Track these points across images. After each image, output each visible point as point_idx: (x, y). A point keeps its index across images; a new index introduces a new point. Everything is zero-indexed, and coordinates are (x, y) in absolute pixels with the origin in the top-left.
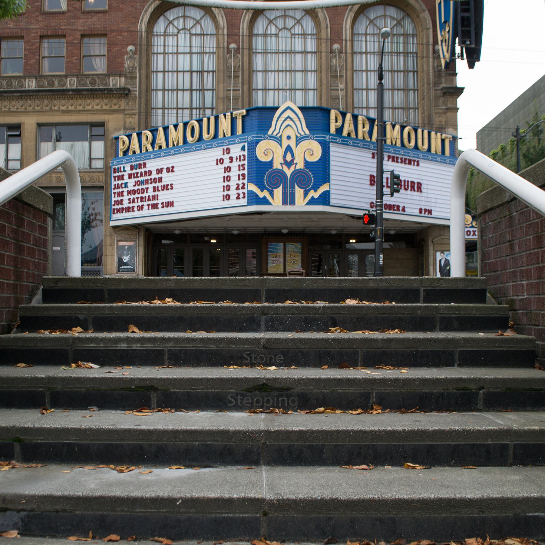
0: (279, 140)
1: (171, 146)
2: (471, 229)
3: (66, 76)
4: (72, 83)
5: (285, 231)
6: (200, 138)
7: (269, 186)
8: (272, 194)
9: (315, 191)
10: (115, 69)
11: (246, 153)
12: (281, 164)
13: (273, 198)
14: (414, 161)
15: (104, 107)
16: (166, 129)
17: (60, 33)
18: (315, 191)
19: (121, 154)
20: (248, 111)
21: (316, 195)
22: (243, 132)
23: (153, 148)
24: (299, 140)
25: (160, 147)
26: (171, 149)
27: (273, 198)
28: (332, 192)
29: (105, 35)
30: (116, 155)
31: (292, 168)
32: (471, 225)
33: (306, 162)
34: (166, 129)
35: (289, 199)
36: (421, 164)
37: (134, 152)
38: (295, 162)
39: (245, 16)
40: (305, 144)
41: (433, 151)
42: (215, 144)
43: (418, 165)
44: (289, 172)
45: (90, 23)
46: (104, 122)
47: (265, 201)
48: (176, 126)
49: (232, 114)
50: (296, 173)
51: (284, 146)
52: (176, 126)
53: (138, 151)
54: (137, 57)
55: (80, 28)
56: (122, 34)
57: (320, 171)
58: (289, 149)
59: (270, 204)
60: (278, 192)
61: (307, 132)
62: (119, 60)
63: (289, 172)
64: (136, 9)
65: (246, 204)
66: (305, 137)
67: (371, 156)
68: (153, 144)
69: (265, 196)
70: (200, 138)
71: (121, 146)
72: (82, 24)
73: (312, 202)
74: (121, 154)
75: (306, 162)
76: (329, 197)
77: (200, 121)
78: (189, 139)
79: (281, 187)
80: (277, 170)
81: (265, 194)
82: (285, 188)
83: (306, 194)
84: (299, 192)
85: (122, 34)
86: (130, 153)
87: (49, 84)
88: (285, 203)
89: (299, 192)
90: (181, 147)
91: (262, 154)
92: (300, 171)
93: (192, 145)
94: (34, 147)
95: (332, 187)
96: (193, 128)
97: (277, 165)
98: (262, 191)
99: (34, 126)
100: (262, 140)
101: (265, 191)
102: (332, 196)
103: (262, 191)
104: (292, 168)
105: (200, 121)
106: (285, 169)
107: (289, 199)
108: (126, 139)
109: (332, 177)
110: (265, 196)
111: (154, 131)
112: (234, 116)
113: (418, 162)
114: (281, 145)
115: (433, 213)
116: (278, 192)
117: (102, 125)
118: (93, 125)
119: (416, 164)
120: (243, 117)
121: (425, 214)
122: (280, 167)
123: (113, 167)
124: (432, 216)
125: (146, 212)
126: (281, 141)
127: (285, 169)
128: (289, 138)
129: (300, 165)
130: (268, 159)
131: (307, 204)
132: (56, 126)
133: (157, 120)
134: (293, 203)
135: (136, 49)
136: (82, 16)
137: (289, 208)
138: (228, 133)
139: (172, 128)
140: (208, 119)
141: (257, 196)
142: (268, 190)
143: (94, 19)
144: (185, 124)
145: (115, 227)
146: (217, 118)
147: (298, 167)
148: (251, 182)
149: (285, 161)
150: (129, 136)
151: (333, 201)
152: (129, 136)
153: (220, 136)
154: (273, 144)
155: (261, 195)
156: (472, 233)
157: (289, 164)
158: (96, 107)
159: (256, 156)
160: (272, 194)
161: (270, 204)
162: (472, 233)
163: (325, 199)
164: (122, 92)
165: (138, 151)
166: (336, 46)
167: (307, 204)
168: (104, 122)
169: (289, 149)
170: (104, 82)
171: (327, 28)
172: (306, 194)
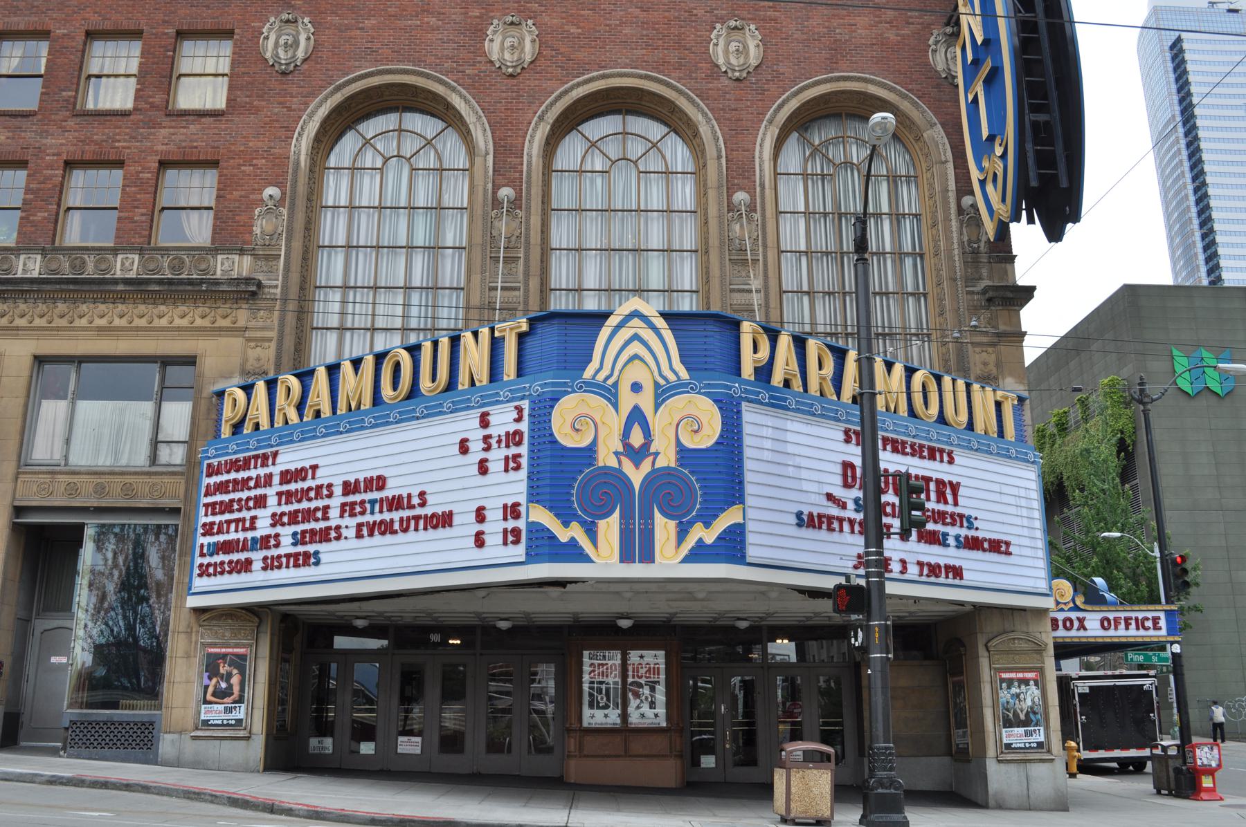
0: (610, 393)
1: (342, 409)
2: (1073, 615)
3: (115, 251)
4: (127, 266)
5: (625, 624)
6: (414, 392)
7: (585, 511)
8: (591, 532)
9: (707, 525)
10: (231, 234)
11: (524, 426)
12: (616, 453)
13: (594, 542)
14: (941, 451)
15: (199, 322)
16: (333, 370)
17: (112, 157)
18: (707, 525)
19: (226, 431)
20: (532, 322)
21: (710, 537)
22: (520, 373)
23: (301, 416)
24: (663, 394)
25: (318, 414)
26: (343, 417)
27: (594, 542)
28: (750, 526)
29: (213, 164)
30: (217, 434)
31: (646, 466)
32: (1071, 605)
33: (682, 451)
34: (333, 370)
35: (637, 546)
36: (957, 459)
37: (257, 426)
38: (652, 450)
39: (535, 130)
40: (678, 404)
41: (979, 427)
42: (447, 404)
44: (636, 476)
45: (183, 137)
46: (195, 357)
47: (573, 552)
48: (357, 363)
49: (492, 330)
50: (656, 478)
51: (626, 406)
52: (357, 363)
53: (265, 424)
54: (285, 211)
55: (160, 148)
56: (255, 162)
57: (717, 475)
58: (637, 416)
59: (586, 559)
60: (610, 527)
61: (684, 374)
62: (243, 218)
63: (636, 476)
64: (289, 109)
65: (523, 559)
66: (678, 388)
67: (842, 436)
68: (300, 408)
69: (573, 539)
70: (414, 392)
71: (227, 412)
72: (165, 139)
73: (700, 553)
74: (226, 431)
75: (682, 451)
76: (743, 542)
77: (414, 350)
78: (387, 391)
79: (616, 514)
80: (607, 471)
81: (576, 532)
82: (626, 518)
83: (682, 534)
84: (664, 528)
85: (255, 162)
86: (248, 429)
87: (73, 267)
88: (626, 556)
89: (664, 528)
90: (366, 412)
91: (569, 430)
92: (667, 471)
93: (392, 407)
94: (20, 410)
95: (751, 514)
96: (397, 366)
97: (606, 457)
98: (566, 524)
99: (27, 362)
100: (567, 393)
101: (574, 524)
102: (750, 538)
103: (566, 524)
104: (646, 466)
105: (414, 350)
106: (628, 468)
107: (637, 546)
108: (240, 395)
109: (749, 489)
110: (573, 539)
111: (305, 376)
112: (497, 334)
113: (950, 454)
114: (616, 406)
115: (965, 574)
116: (610, 527)
117: (190, 361)
118: (166, 361)
119: (946, 458)
120: (521, 337)
121: (947, 577)
122: (612, 462)
123: (207, 462)
124: (963, 583)
125: (257, 576)
126: (616, 395)
127: (628, 468)
128: (636, 387)
129: (667, 459)
130: (584, 442)
131: (686, 560)
132: (80, 362)
133: (324, 349)
134: (648, 556)
135: (284, 194)
136: (166, 122)
137: (637, 570)
138: (483, 377)
139: (347, 367)
140: (435, 344)
141: (553, 537)
142: (583, 523)
143: (193, 128)
144: (380, 358)
145: (199, 611)
146: (455, 341)
147: (660, 463)
148: (538, 502)
149: (627, 445)
150: (248, 389)
151: (752, 553)
152: (248, 389)
153: (463, 383)
154: (595, 404)
155: (563, 535)
156: (1076, 624)
157: (637, 455)
158: (178, 322)
159: (552, 435)
160: (591, 532)
161: (586, 559)
162: (1076, 624)
163: (732, 546)
164: (243, 287)
165: (265, 424)
166: (740, 196)
167: (686, 560)
168: (195, 357)
169: (637, 416)
170: (203, 267)
171: (719, 157)
172: (682, 534)
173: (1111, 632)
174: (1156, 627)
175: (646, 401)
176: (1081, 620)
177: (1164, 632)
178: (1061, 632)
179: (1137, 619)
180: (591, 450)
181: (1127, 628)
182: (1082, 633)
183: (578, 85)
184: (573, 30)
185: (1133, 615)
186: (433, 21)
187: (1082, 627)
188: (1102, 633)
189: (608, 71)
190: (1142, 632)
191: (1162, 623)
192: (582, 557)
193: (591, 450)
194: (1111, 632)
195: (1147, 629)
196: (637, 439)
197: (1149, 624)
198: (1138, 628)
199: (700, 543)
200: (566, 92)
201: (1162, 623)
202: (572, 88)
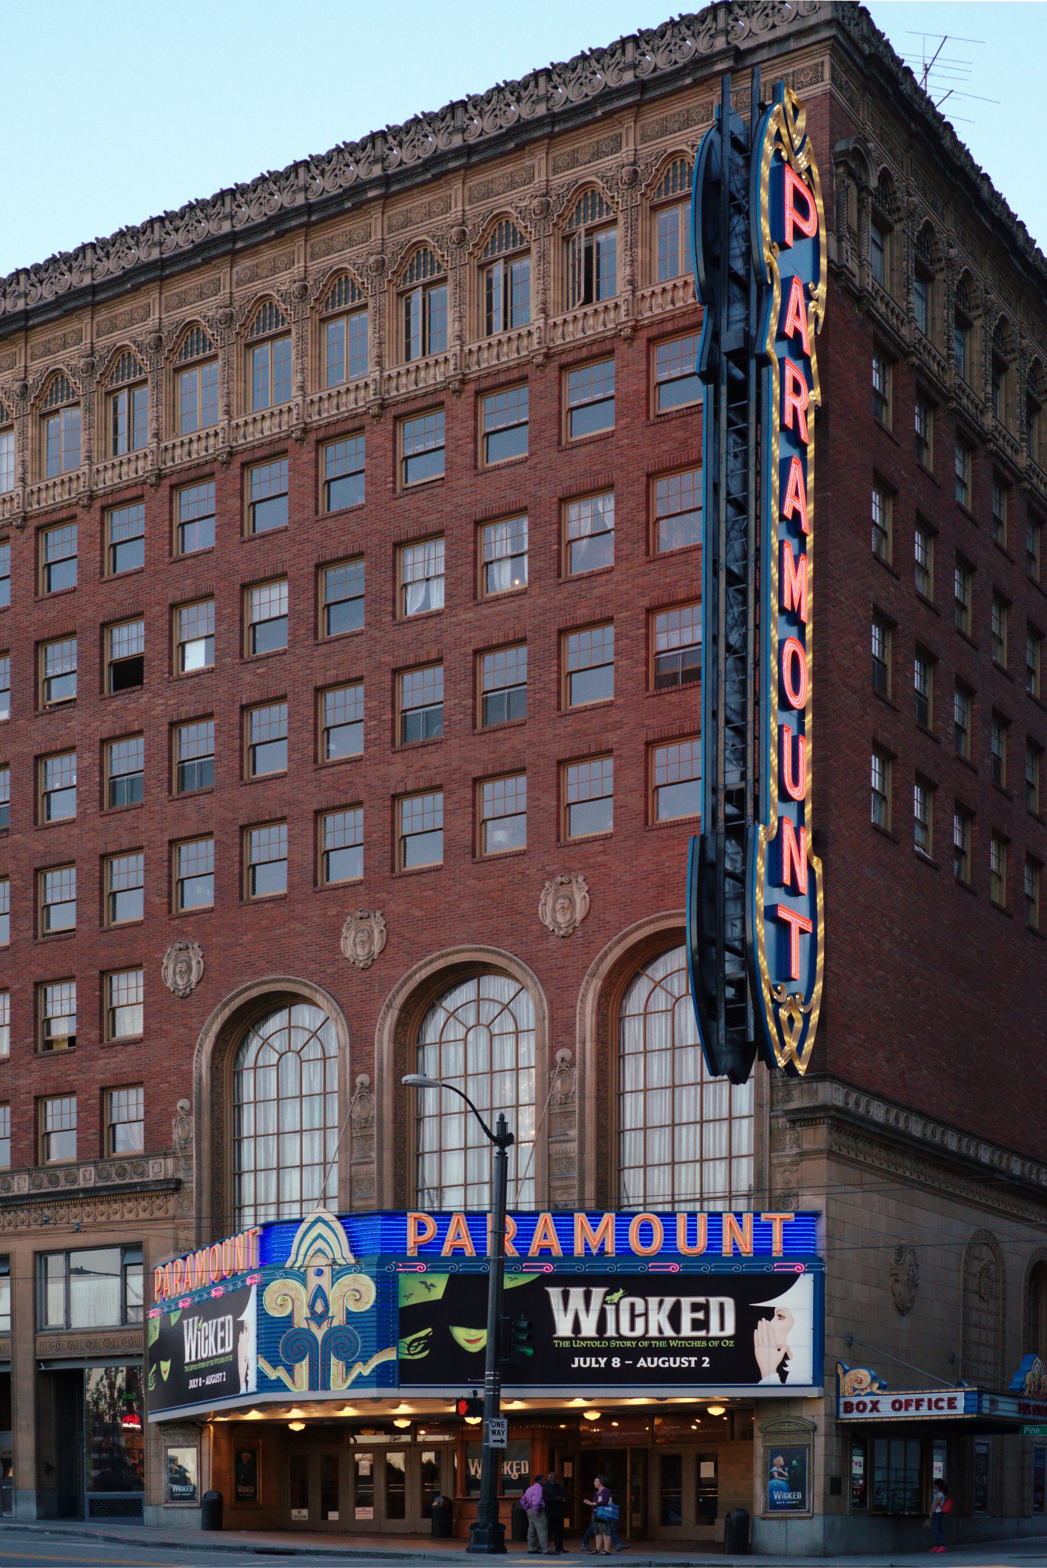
7: (286, 1357)
8: (290, 1371)
9: (365, 1362)
12: (307, 1319)
13: (292, 1377)
18: (365, 1362)
27: (292, 1377)
31: (325, 1327)
38: (330, 1314)
40: (347, 1281)
44: (319, 1334)
60: (303, 1369)
63: (319, 1334)
75: (349, 1313)
79: (307, 1359)
80: (301, 1331)
81: (280, 1373)
83: (349, 1367)
84: (336, 1366)
89: (336, 1366)
92: (339, 1329)
97: (301, 1321)
98: (275, 1367)
103: (275, 1367)
104: (325, 1327)
106: (314, 1328)
114: (305, 1285)
122: (304, 1325)
134: (326, 1387)
142: (285, 1365)
147: (336, 1323)
157: (318, 1318)
160: (290, 1371)
179: (930, 1400)
180: (290, 1317)
181: (917, 1409)
183: (421, 968)
184: (418, 913)
185: (926, 1397)
186: (298, 926)
189: (444, 951)
192: (284, 1388)
193: (290, 1317)
196: (319, 1308)
198: (930, 1408)
199: (360, 1376)
200: (410, 977)
202: (415, 972)
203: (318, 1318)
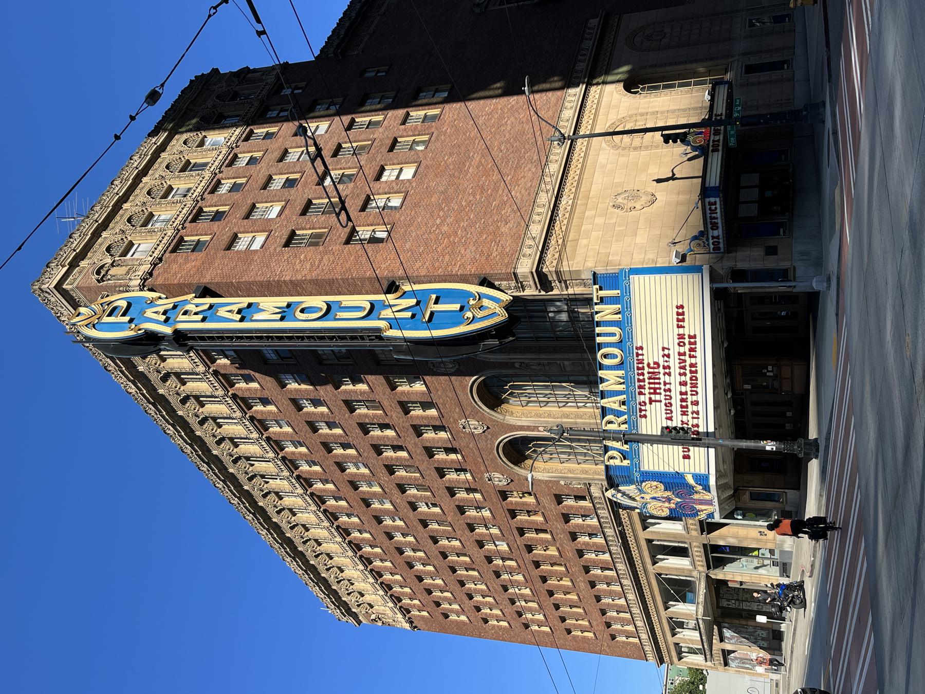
2: (711, 241)
21: (699, 488)
28: (692, 471)
43: (641, 348)
57: (673, 482)
84: (696, 497)
89: (696, 497)
95: (687, 470)
97: (673, 506)
102: (697, 471)
116: (698, 507)
119: (640, 352)
129: (668, 494)
131: (709, 492)
137: (716, 503)
151: (703, 471)
163: (702, 480)
167: (709, 492)
169: (653, 498)
173: (720, 225)
174: (715, 203)
175: (647, 497)
176: (713, 237)
177: (718, 200)
178: (721, 246)
182: (721, 237)
187: (718, 237)
188: (720, 230)
190: (718, 210)
191: (712, 200)
194: (720, 225)
195: (716, 208)
197: (713, 207)
201: (712, 200)
203: (669, 500)
